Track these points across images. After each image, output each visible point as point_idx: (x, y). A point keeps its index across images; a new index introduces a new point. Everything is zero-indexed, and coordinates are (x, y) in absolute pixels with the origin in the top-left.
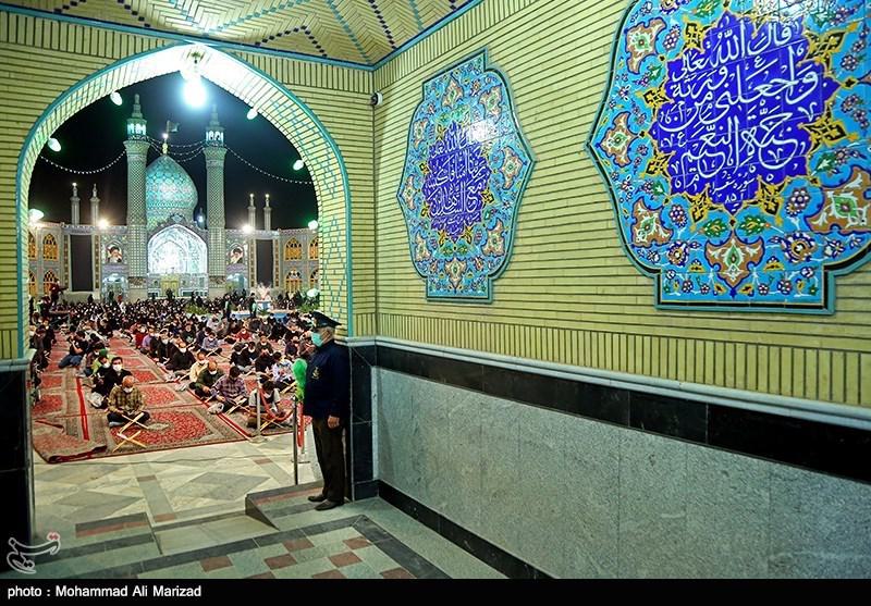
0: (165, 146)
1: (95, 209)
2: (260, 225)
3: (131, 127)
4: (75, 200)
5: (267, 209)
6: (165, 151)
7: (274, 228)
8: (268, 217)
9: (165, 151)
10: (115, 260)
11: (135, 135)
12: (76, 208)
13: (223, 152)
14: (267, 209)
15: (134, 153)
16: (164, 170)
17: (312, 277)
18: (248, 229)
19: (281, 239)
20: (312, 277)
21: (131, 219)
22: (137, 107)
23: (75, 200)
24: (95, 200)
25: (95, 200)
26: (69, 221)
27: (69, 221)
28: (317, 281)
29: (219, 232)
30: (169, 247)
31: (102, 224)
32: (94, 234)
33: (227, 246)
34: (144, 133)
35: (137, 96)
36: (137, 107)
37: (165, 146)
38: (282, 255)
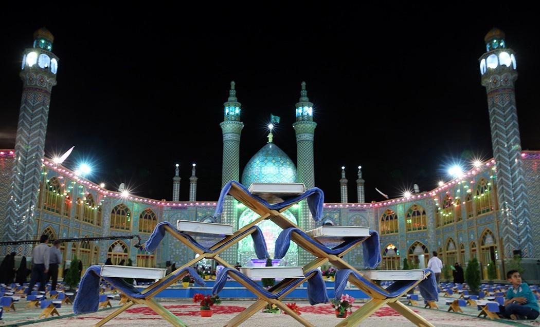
0: (270, 136)
3: (227, 111)
4: (177, 179)
6: (270, 140)
8: (361, 189)
9: (270, 140)
13: (312, 126)
14: (360, 181)
16: (267, 155)
22: (233, 92)
23: (177, 179)
26: (170, 198)
36: (233, 92)
37: (270, 136)
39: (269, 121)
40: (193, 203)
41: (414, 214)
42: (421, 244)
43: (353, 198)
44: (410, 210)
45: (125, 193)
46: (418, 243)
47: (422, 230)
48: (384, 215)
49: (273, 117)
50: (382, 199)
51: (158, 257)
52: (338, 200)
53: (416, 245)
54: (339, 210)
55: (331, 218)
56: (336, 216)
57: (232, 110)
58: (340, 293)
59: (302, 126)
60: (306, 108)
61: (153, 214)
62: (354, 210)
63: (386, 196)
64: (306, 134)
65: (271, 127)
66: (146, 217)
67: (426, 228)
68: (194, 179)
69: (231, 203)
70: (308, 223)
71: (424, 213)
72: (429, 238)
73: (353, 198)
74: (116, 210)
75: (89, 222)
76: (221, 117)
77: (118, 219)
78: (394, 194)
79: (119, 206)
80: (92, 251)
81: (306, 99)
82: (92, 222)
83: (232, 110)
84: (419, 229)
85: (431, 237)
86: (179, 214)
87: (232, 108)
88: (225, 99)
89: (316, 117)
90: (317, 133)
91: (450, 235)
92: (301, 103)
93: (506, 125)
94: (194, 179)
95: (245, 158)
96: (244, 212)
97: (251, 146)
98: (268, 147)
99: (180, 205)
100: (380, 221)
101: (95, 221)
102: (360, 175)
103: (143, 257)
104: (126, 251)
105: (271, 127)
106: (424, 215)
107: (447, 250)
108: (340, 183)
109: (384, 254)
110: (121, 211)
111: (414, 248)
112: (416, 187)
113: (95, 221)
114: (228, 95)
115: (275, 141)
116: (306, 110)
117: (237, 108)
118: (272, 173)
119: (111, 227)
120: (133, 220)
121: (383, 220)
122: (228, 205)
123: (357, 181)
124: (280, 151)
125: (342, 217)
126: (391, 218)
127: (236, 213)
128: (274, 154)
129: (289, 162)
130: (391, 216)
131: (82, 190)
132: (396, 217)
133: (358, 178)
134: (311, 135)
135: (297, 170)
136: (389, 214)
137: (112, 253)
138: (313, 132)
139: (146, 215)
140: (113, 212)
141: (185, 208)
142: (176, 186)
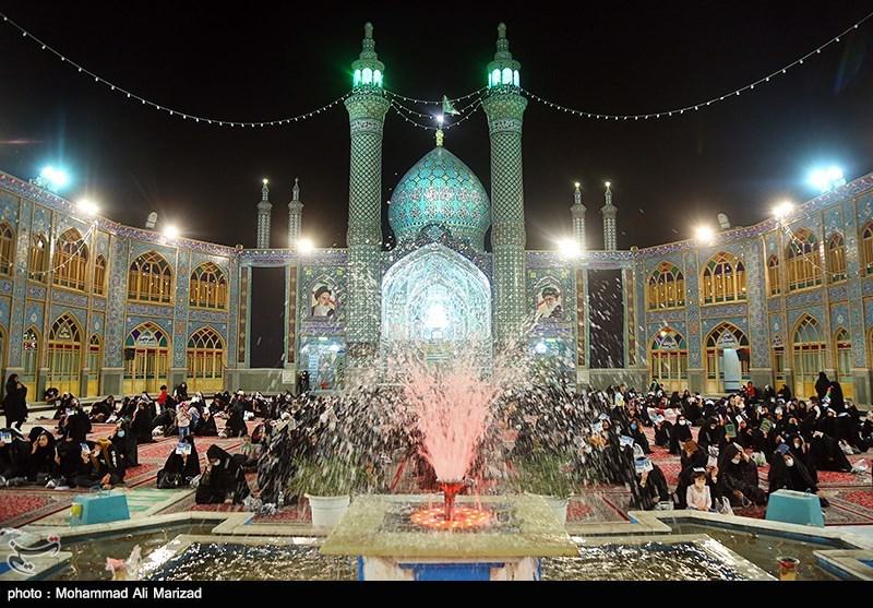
0: (439, 135)
1: (295, 219)
2: (597, 242)
4: (265, 206)
5: (609, 208)
6: (439, 142)
7: (623, 245)
8: (610, 226)
9: (439, 142)
10: (323, 311)
11: (362, 87)
12: (264, 222)
13: (519, 105)
14: (609, 208)
15: (363, 121)
17: (710, 343)
18: (570, 249)
19: (638, 270)
20: (710, 343)
21: (353, 237)
23: (265, 206)
24: (295, 206)
25: (295, 206)
26: (251, 243)
27: (251, 243)
28: (721, 352)
31: (304, 245)
32: (289, 263)
33: (529, 290)
34: (380, 85)
37: (439, 135)
38: (641, 300)
41: (718, 271)
42: (732, 328)
44: (711, 264)
45: (170, 234)
46: (727, 325)
53: (721, 329)
57: (367, 76)
58: (627, 460)
59: (500, 104)
60: (507, 72)
64: (507, 124)
65: (440, 119)
67: (745, 298)
70: (512, 287)
71: (741, 268)
72: (751, 316)
74: (140, 264)
75: (74, 286)
76: (346, 88)
77: (145, 281)
79: (146, 256)
80: (84, 344)
81: (504, 54)
82: (81, 288)
83: (367, 76)
84: (717, 300)
85: (754, 314)
87: (367, 71)
88: (354, 53)
90: (529, 118)
91: (812, 312)
92: (496, 63)
97: (403, 150)
98: (436, 154)
101: (90, 286)
104: (164, 343)
105: (440, 119)
106: (740, 273)
107: (796, 341)
111: (716, 335)
113: (90, 286)
115: (446, 144)
116: (503, 76)
117: (377, 72)
119: (130, 297)
120: (179, 286)
124: (457, 160)
126: (670, 278)
128: (445, 167)
129: (472, 179)
130: (668, 274)
132: (680, 277)
133: (605, 204)
134: (518, 122)
136: (665, 270)
138: (521, 117)
139: (205, 274)
140: (134, 267)
142: (263, 220)
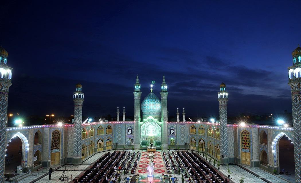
0: (152, 90)
6: (152, 91)
8: (184, 116)
9: (152, 91)
13: (166, 94)
15: (137, 95)
26: (116, 120)
29: (164, 122)
30: (151, 127)
35: (138, 76)
37: (152, 90)
39: (151, 83)
40: (124, 122)
41: (201, 129)
43: (181, 120)
47: (203, 135)
48: (192, 127)
49: (152, 81)
50: (190, 121)
51: (113, 141)
52: (176, 121)
54: (176, 124)
55: (173, 127)
56: (175, 126)
61: (110, 127)
62: (181, 124)
63: (191, 120)
65: (152, 86)
66: (108, 128)
68: (124, 113)
69: (138, 122)
71: (204, 129)
73: (181, 120)
76: (133, 90)
77: (99, 131)
78: (195, 120)
81: (164, 83)
86: (119, 126)
89: (169, 90)
90: (169, 95)
93: (223, 114)
94: (124, 113)
95: (142, 99)
96: (142, 125)
99: (120, 123)
100: (190, 128)
102: (184, 111)
103: (108, 142)
104: (102, 141)
108: (176, 114)
109: (191, 140)
110: (100, 128)
112: (202, 119)
114: (136, 81)
118: (153, 106)
121: (191, 128)
122: (136, 129)
123: (183, 113)
125: (177, 126)
127: (139, 126)
131: (90, 127)
135: (161, 103)
137: (98, 143)
140: (98, 129)
141: (121, 124)
